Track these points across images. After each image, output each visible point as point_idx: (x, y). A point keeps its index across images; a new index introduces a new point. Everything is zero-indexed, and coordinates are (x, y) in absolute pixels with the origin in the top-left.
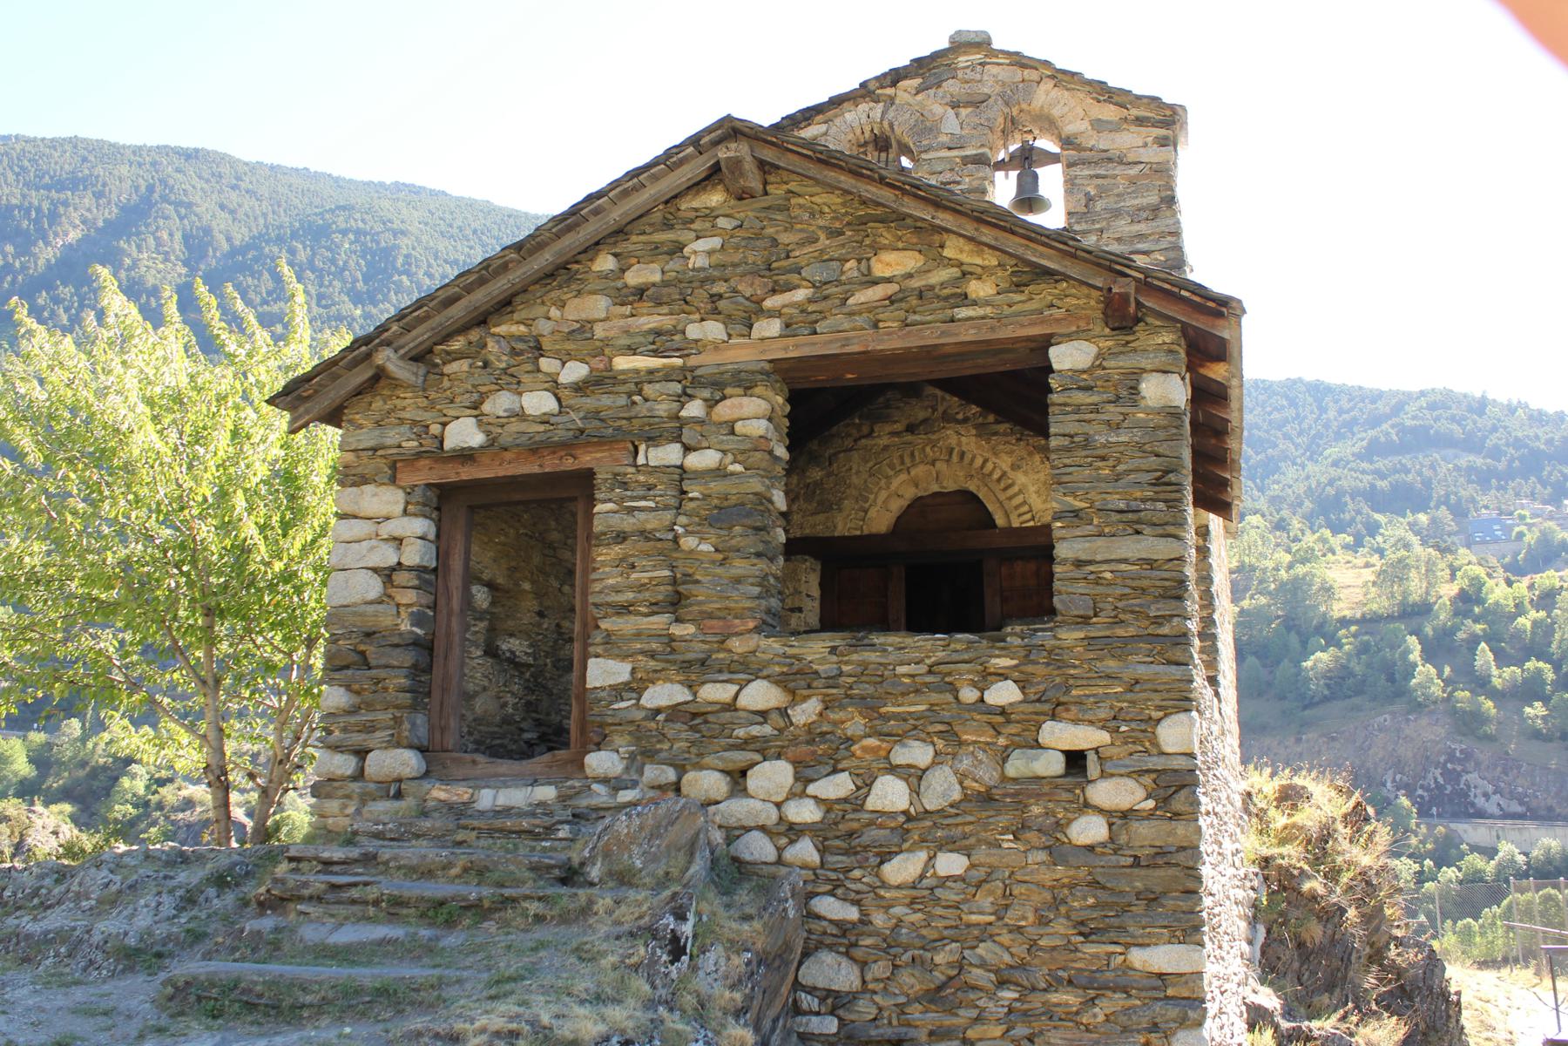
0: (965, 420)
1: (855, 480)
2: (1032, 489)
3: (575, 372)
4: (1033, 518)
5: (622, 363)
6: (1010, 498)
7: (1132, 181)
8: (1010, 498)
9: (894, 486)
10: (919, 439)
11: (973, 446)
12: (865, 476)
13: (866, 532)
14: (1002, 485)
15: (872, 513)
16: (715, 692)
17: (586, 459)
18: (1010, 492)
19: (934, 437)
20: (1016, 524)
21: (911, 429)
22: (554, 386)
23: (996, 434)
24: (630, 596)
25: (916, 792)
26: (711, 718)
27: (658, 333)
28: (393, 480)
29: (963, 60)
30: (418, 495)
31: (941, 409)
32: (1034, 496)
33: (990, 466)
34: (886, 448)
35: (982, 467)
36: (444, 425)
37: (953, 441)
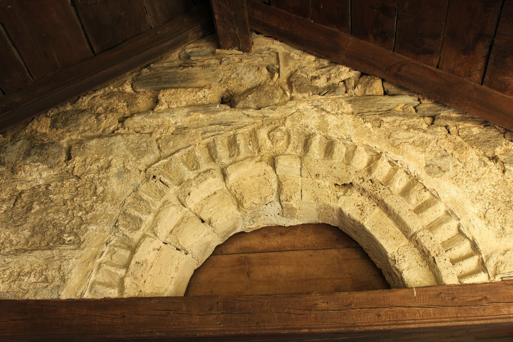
0: (331, 89)
1: (115, 186)
2: (473, 210)
4: (482, 267)
6: (431, 228)
8: (431, 228)
9: (194, 201)
10: (243, 118)
11: (350, 131)
12: (137, 179)
13: (130, 292)
14: (414, 202)
15: (146, 252)
18: (431, 215)
19: (276, 114)
20: (450, 278)
21: (229, 100)
23: (389, 112)
31: (285, 72)
32: (480, 223)
33: (383, 169)
34: (181, 131)
35: (369, 170)
37: (312, 120)
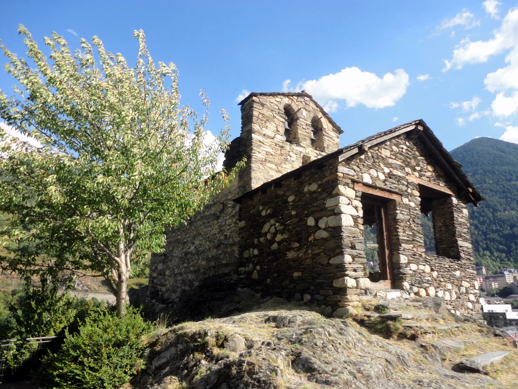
3: (387, 170)
5: (395, 172)
7: (334, 144)
16: (421, 267)
17: (394, 197)
22: (384, 173)
24: (406, 238)
25: (451, 296)
26: (422, 274)
27: (400, 165)
28: (353, 189)
29: (306, 98)
30: (360, 194)
36: (362, 173)
